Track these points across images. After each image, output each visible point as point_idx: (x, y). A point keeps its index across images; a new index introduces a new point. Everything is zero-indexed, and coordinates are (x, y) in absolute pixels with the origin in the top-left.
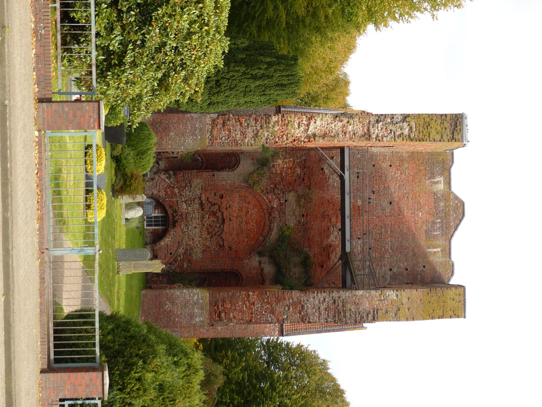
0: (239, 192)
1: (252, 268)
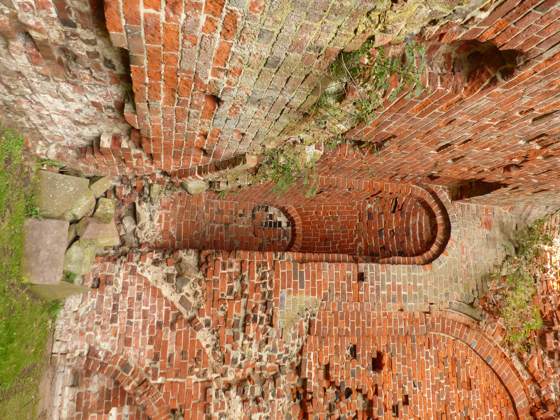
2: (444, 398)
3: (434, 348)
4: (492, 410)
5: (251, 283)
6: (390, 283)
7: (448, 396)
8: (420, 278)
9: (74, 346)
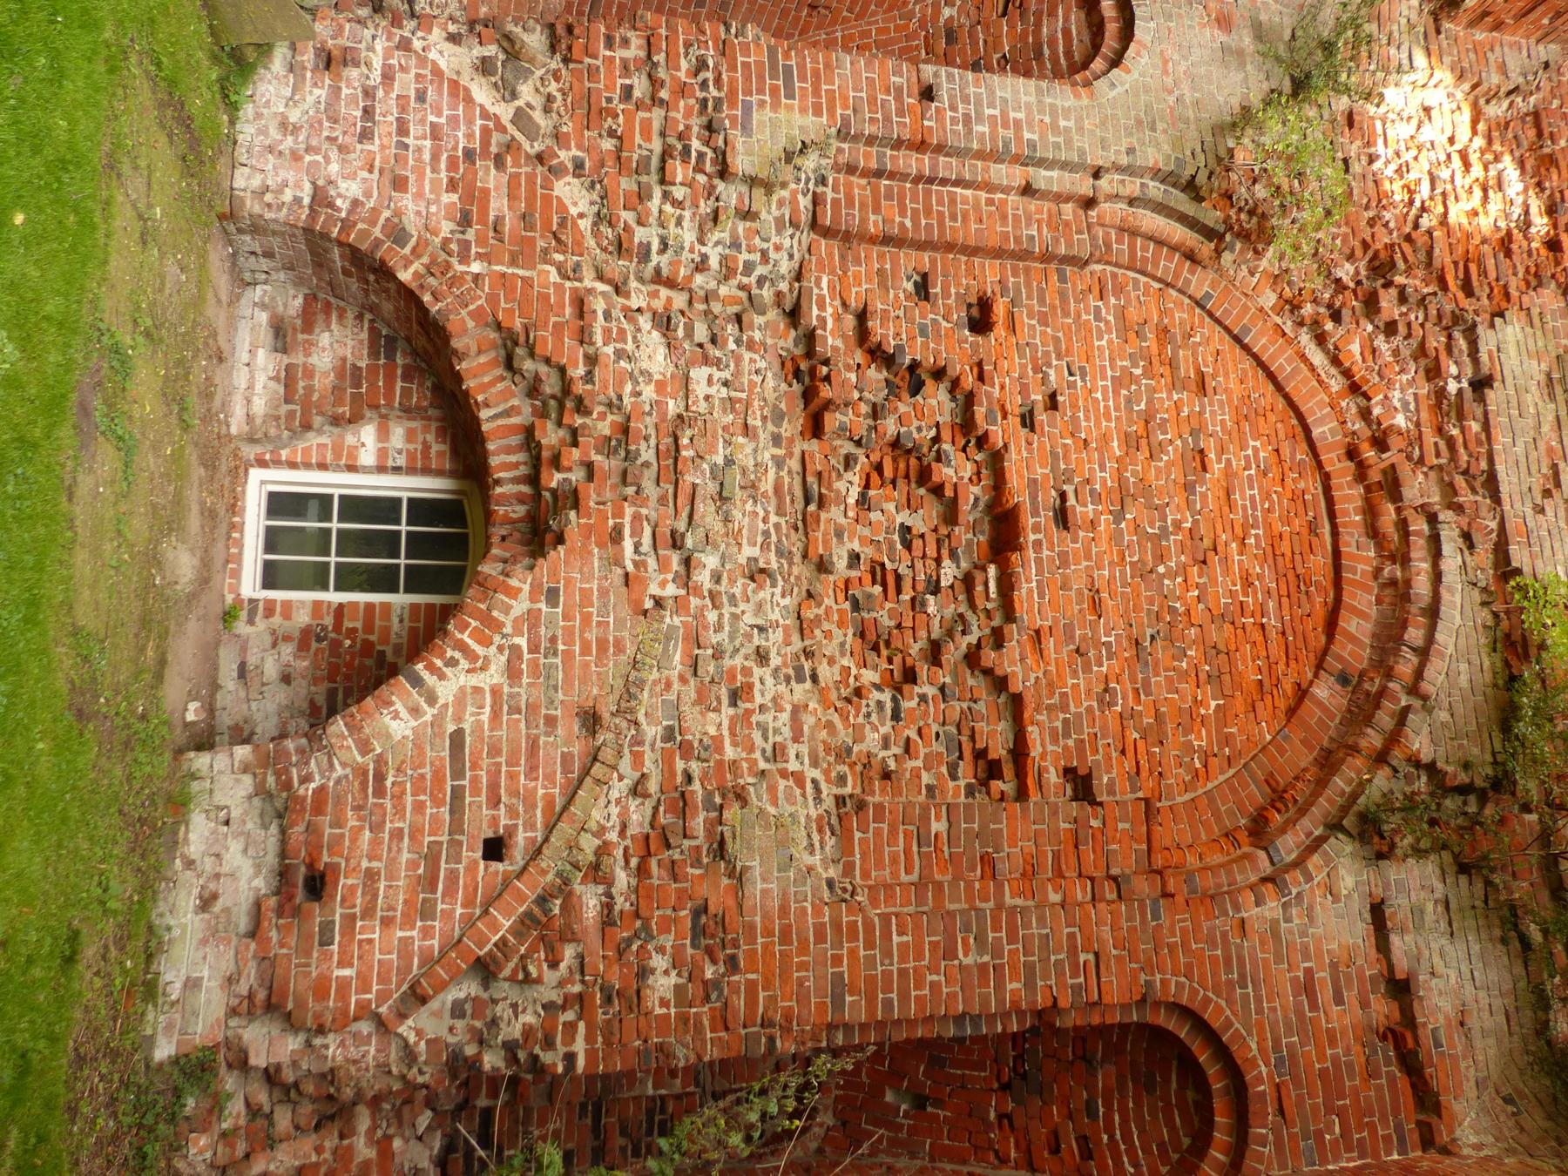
0: (1119, 290)
1: (1323, 975)
2: (1143, 406)
3: (1113, 301)
4: (1258, 444)
5: (673, 78)
6: (997, 112)
7: (1150, 402)
8: (1067, 112)
9: (279, 180)
